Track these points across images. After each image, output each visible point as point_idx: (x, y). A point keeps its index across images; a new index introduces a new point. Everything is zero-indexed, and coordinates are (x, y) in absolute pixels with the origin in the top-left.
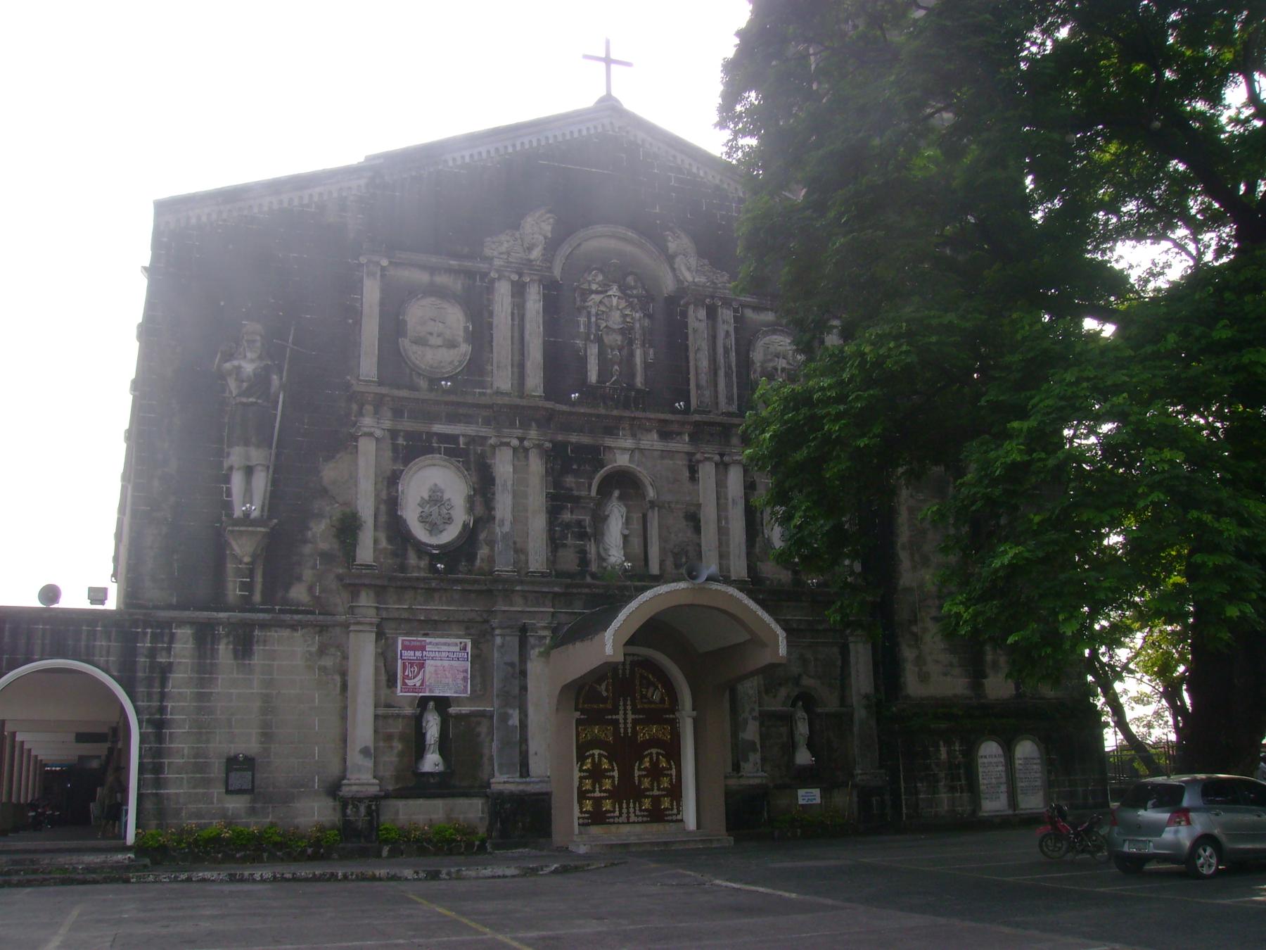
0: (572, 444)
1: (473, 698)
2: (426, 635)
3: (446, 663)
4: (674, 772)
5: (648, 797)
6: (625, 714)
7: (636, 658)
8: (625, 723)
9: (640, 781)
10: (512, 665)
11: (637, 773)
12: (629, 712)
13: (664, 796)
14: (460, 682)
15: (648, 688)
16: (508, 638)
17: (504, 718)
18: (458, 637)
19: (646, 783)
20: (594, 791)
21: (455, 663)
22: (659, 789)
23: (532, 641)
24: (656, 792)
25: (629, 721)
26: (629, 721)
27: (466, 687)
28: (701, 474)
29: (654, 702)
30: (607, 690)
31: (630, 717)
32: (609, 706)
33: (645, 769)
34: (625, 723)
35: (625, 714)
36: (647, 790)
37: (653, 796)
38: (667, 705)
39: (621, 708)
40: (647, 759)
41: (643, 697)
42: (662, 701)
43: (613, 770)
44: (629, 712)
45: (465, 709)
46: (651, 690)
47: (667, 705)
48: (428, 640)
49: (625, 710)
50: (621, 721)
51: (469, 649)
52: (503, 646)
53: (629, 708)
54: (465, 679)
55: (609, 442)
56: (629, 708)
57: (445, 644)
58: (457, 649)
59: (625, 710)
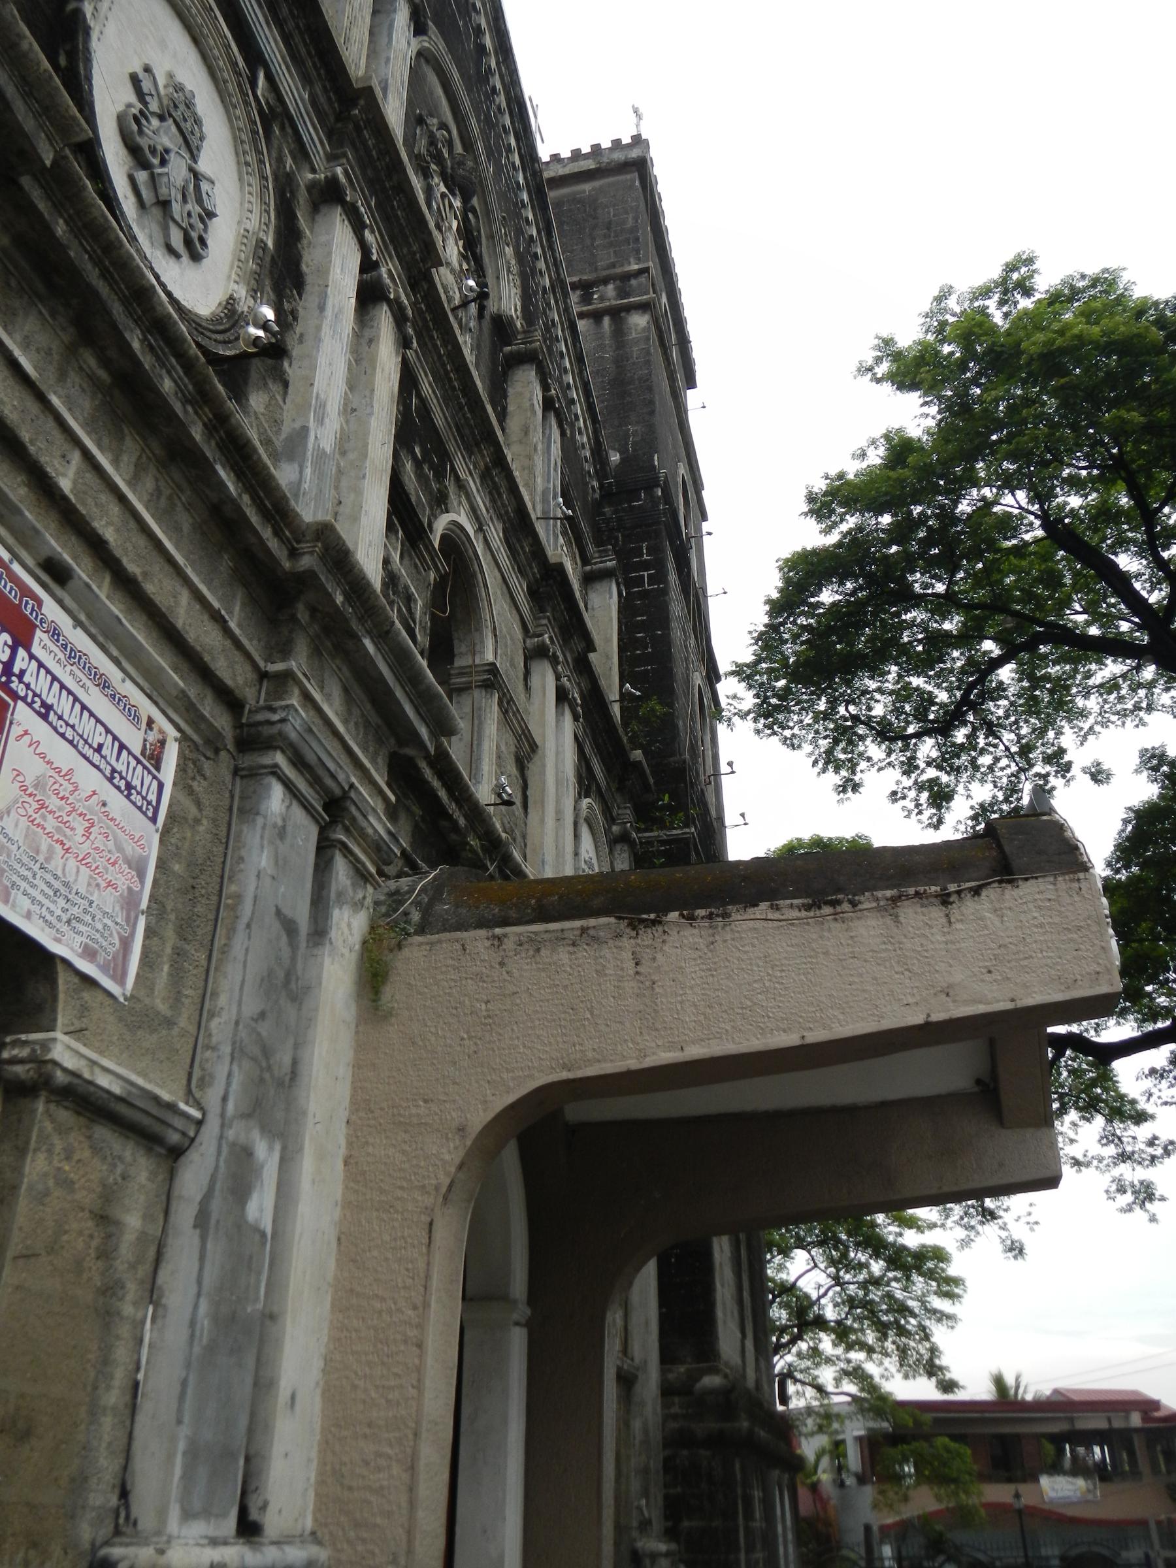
0: (419, 395)
1: (136, 1018)
2: (56, 573)
3: (90, 779)
10: (290, 927)
14: (108, 900)
16: (298, 813)
17: (240, 1175)
18: (155, 689)
21: (117, 802)
23: (341, 869)
27: (126, 944)
28: (535, 681)
45: (112, 1073)
48: (51, 610)
51: (168, 772)
52: (282, 833)
54: (130, 901)
55: (461, 465)
57: (104, 684)
58: (134, 739)
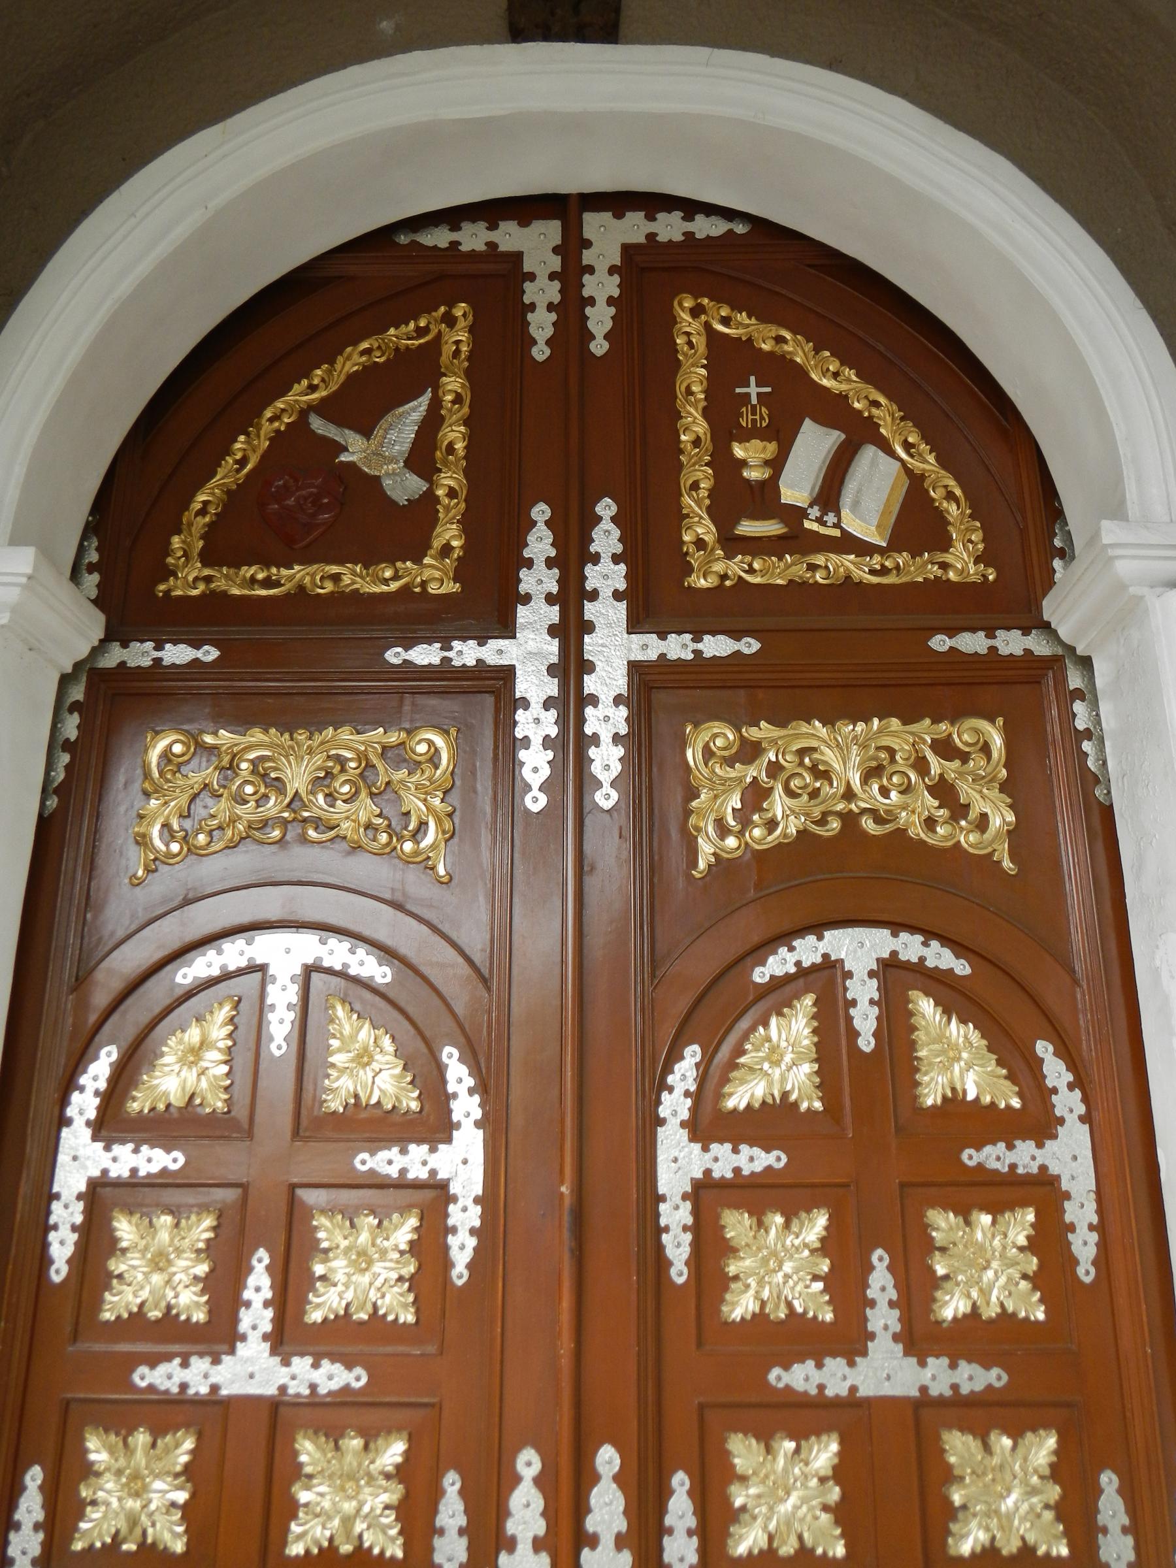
4: (1070, 1156)
5: (804, 1416)
6: (571, 630)
7: (670, 227)
8: (572, 702)
9: (709, 1246)
11: (679, 1161)
12: (607, 615)
13: (978, 1414)
15: (782, 436)
19: (779, 1268)
20: (219, 1335)
22: (920, 1337)
24: (885, 1371)
25: (607, 680)
26: (607, 680)
29: (848, 544)
30: (422, 457)
31: (615, 649)
32: (435, 576)
33: (768, 1122)
34: (572, 702)
35: (571, 630)
36: (797, 1337)
37: (850, 1417)
38: (962, 561)
39: (538, 580)
40: (794, 1029)
41: (737, 497)
42: (917, 525)
43: (435, 1126)
44: (607, 615)
46: (814, 444)
47: (962, 561)
49: (572, 597)
50: (535, 685)
53: (606, 576)
56: (606, 576)
59: (572, 597)
